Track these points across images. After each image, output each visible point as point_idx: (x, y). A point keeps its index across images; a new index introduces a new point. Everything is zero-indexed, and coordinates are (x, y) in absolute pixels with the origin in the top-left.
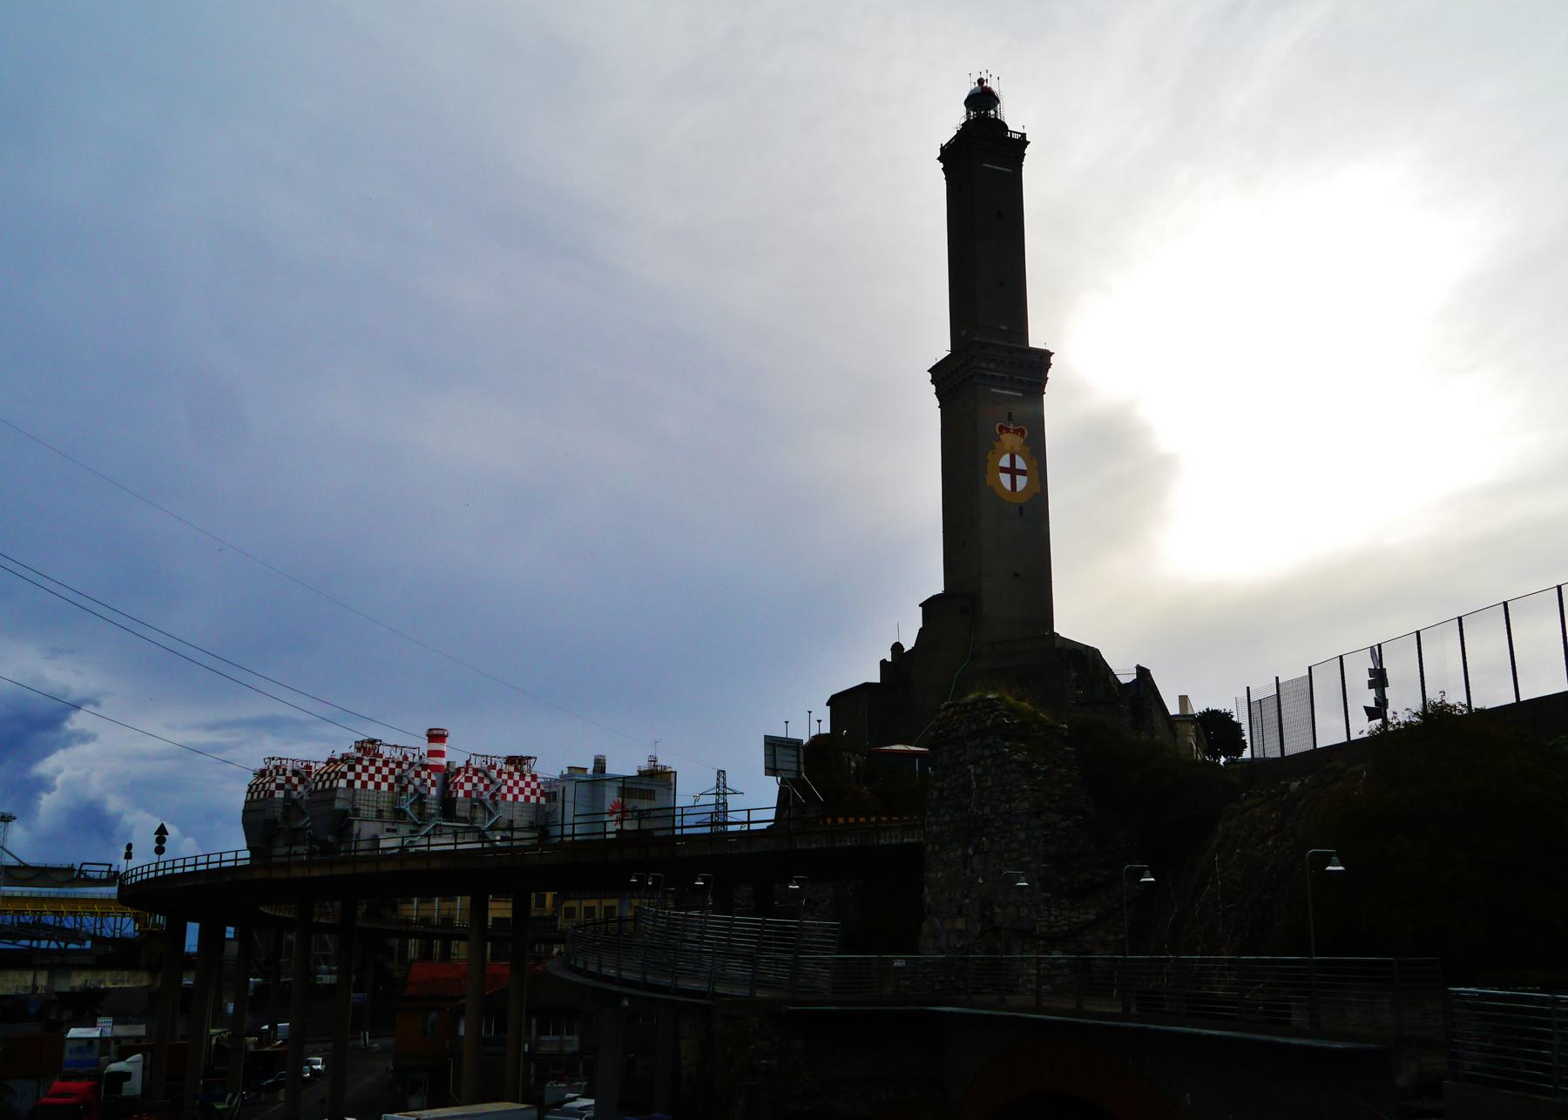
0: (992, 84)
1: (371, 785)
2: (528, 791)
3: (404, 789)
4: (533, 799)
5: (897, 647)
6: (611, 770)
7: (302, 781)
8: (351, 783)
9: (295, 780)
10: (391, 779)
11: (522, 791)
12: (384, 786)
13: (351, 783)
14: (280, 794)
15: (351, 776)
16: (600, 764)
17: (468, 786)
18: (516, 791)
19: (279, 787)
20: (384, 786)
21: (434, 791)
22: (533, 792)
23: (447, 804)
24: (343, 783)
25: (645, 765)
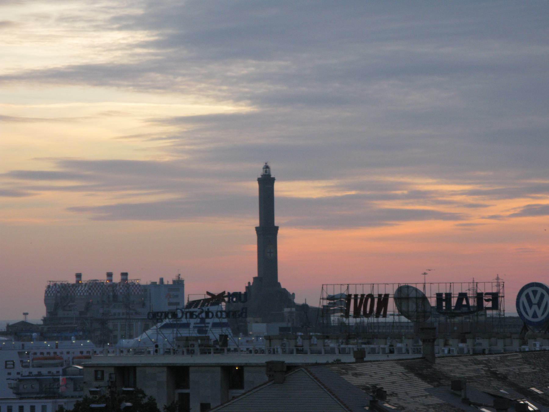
0: (269, 165)
1: (95, 294)
2: (138, 291)
3: (104, 294)
4: (140, 293)
5: (249, 283)
6: (165, 283)
7: (64, 289)
8: (90, 294)
9: (62, 289)
10: (100, 291)
11: (136, 291)
12: (99, 294)
13: (90, 294)
14: (59, 295)
15: (90, 291)
16: (162, 280)
17: (121, 291)
18: (135, 291)
19: (58, 292)
20: (99, 294)
21: (111, 294)
22: (140, 290)
23: (115, 296)
24: (88, 294)
25: (175, 278)
